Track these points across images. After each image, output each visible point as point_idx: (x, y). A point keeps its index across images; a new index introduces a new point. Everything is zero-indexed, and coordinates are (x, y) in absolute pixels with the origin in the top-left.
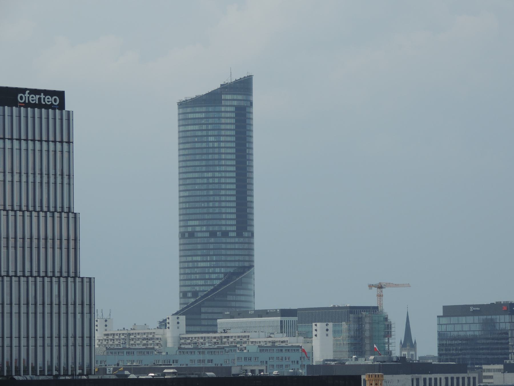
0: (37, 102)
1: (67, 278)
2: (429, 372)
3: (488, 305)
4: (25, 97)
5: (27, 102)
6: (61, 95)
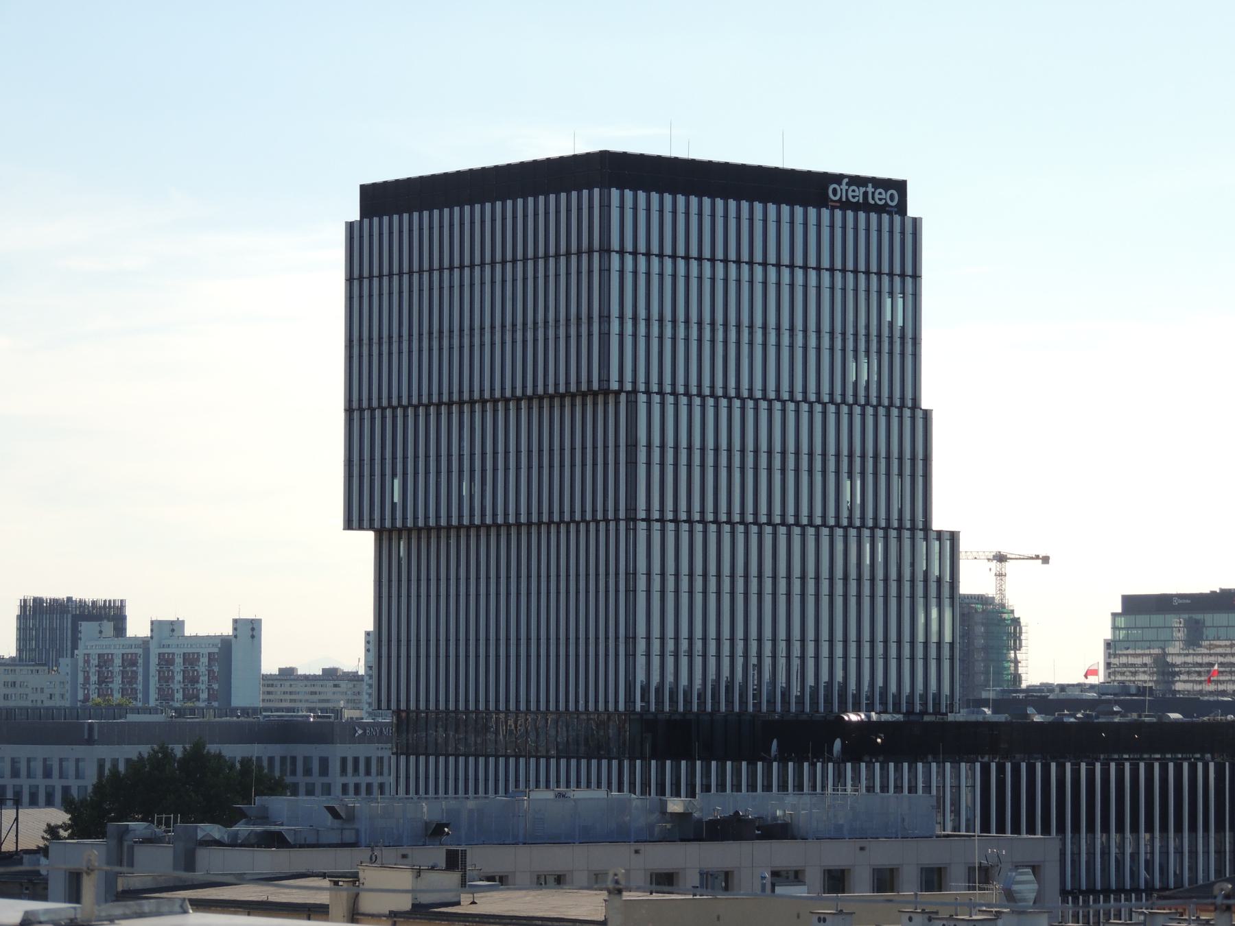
0: (861, 201)
1: (872, 529)
2: (1195, 715)
3: (1206, 594)
4: (841, 190)
5: (844, 199)
6: (900, 187)
